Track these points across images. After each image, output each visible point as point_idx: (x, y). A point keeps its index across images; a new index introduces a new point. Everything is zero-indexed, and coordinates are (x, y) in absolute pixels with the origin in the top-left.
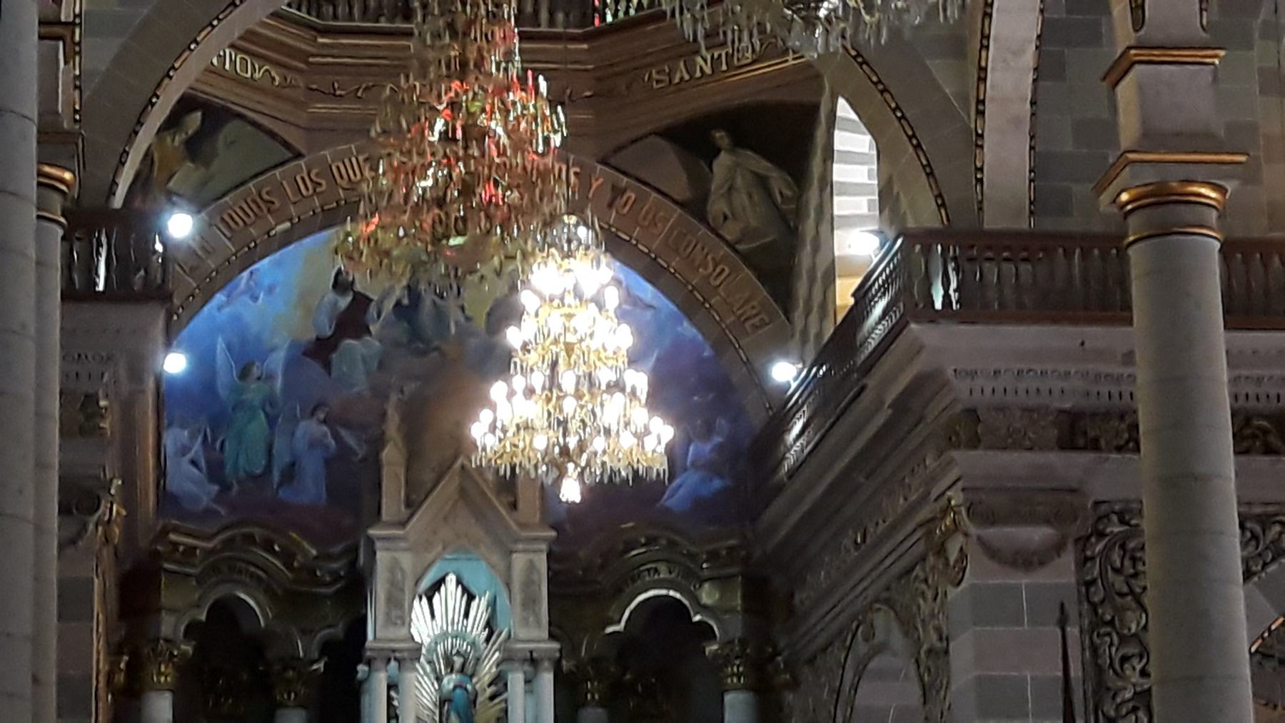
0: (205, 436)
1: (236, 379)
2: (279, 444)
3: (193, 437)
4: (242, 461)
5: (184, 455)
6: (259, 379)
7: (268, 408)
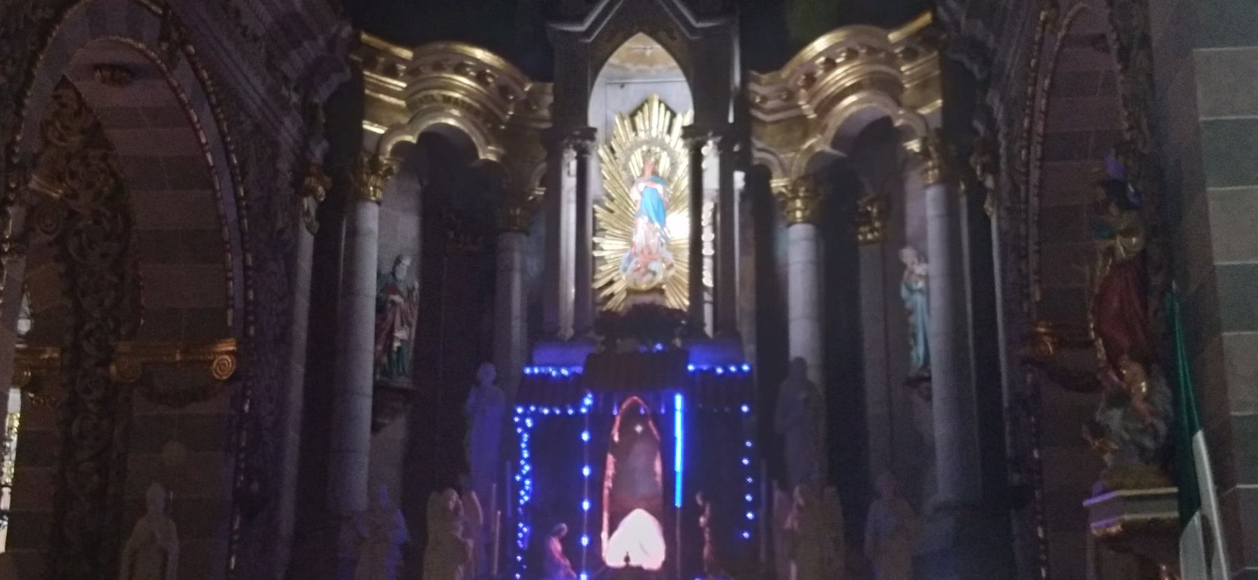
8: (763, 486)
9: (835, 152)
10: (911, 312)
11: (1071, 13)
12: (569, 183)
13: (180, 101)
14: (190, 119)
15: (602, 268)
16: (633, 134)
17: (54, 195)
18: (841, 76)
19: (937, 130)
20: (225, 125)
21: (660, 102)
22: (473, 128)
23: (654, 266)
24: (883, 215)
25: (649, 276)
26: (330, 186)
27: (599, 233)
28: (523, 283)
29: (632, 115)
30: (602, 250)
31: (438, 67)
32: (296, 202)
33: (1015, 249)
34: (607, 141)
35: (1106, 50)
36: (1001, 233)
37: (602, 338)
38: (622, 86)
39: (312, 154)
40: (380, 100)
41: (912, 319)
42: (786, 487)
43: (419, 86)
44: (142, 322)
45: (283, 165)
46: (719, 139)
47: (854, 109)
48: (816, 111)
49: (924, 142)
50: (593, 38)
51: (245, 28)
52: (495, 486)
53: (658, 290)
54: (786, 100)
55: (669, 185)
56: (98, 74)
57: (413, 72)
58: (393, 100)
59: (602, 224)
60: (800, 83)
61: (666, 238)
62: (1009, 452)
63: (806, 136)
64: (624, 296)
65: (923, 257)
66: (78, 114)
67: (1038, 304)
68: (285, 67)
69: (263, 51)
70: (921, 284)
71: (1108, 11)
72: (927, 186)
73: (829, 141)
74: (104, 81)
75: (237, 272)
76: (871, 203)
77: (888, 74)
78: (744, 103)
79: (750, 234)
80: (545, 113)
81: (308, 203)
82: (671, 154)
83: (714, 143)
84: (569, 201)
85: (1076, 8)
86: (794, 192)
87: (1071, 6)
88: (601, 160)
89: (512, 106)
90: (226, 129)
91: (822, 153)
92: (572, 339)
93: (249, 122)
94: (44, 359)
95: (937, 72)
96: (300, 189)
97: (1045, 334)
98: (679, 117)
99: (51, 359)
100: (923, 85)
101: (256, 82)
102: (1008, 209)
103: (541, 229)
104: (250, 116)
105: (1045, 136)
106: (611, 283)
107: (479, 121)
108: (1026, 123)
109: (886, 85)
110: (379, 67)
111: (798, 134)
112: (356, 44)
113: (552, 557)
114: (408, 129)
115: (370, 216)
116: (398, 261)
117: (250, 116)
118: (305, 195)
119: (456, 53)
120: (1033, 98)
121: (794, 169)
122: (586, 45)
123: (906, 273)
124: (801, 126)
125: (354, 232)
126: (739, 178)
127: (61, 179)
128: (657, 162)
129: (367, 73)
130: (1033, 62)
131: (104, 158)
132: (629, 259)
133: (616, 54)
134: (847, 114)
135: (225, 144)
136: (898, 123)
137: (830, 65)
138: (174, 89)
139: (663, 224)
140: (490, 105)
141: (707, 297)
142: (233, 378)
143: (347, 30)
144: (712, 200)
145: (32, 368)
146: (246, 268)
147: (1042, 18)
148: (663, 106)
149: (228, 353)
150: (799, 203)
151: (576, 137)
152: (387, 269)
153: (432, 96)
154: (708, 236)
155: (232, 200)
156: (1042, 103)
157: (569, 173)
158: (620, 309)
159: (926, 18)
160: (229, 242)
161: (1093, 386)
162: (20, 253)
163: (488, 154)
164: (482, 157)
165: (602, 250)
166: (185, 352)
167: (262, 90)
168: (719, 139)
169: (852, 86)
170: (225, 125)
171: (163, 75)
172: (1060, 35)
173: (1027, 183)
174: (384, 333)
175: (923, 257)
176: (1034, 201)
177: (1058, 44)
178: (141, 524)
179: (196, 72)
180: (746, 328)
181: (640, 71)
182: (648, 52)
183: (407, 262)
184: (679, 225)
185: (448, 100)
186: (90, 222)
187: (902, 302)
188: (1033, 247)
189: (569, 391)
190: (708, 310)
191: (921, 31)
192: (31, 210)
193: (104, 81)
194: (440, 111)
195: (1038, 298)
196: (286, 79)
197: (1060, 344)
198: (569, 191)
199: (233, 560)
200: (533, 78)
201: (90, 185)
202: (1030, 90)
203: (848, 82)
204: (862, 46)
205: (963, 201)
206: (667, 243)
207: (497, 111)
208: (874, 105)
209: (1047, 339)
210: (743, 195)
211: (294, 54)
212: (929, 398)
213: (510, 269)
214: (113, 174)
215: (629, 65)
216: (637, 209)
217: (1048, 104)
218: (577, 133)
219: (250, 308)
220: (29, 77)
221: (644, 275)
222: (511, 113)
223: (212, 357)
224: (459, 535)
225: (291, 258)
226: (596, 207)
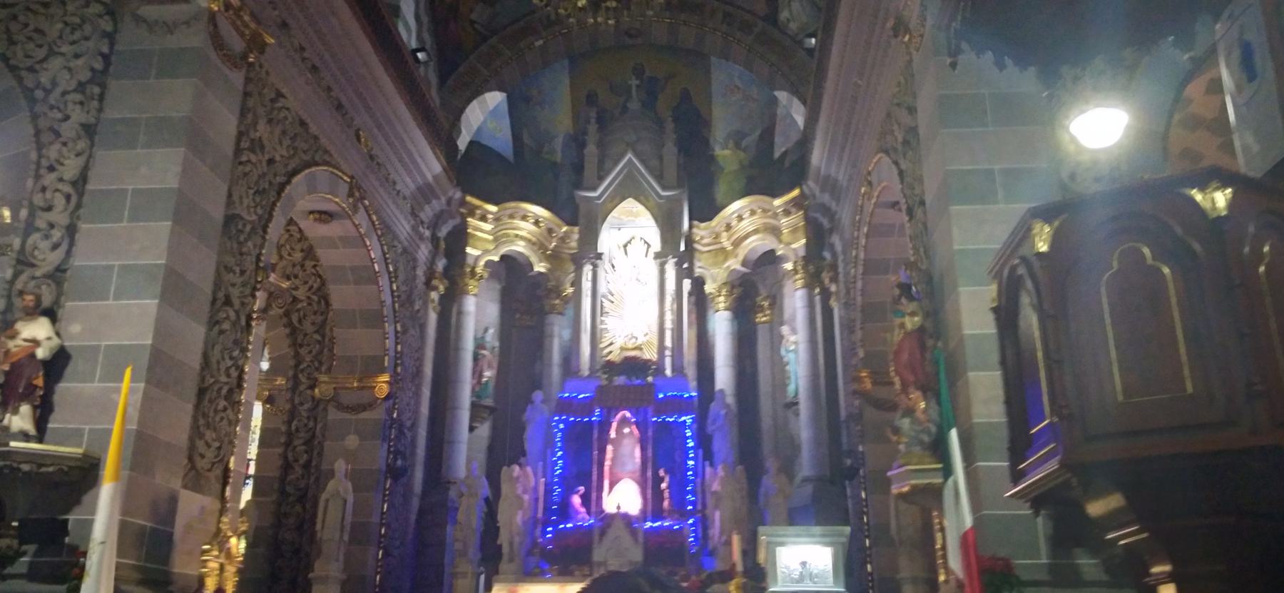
8: (700, 466)
10: (788, 364)
11: (879, 189)
12: (586, 285)
13: (360, 233)
14: (364, 242)
15: (606, 335)
17: (284, 286)
19: (804, 257)
20: (385, 248)
21: (641, 238)
24: (772, 306)
25: (634, 340)
26: (447, 285)
27: (604, 315)
28: (560, 344)
29: (625, 246)
31: (512, 217)
32: (427, 295)
33: (848, 328)
34: (610, 261)
35: (900, 210)
36: (841, 318)
37: (606, 376)
38: (619, 229)
39: (437, 266)
40: (476, 235)
41: (788, 368)
42: (712, 465)
43: (499, 228)
44: (335, 363)
45: (420, 272)
46: (676, 260)
47: (754, 244)
48: (732, 244)
49: (795, 262)
50: (602, 200)
51: (399, 192)
52: (541, 463)
53: (639, 348)
56: (311, 216)
57: (497, 219)
59: (606, 310)
60: (723, 229)
62: (845, 447)
63: (726, 259)
64: (619, 352)
65: (794, 331)
66: (300, 240)
67: (862, 359)
68: (422, 215)
69: (409, 205)
70: (792, 347)
71: (900, 186)
73: (740, 262)
74: (315, 220)
75: (391, 335)
76: (764, 299)
78: (690, 242)
79: (694, 316)
80: (574, 244)
81: (434, 295)
84: (587, 296)
85: (883, 185)
86: (719, 291)
87: (879, 185)
88: (607, 273)
89: (555, 239)
90: (386, 251)
91: (734, 270)
92: (589, 376)
93: (400, 246)
94: (276, 385)
96: (429, 285)
97: (865, 377)
99: (279, 385)
100: (794, 230)
101: (404, 223)
103: (570, 312)
104: (400, 242)
105: (865, 260)
106: (611, 344)
107: (535, 248)
108: (854, 253)
109: (775, 231)
110: (478, 216)
111: (721, 258)
112: (463, 203)
113: (573, 507)
114: (493, 252)
115: (470, 304)
116: (486, 330)
117: (400, 242)
119: (519, 208)
120: (858, 238)
121: (719, 279)
122: (597, 204)
123: (784, 341)
124: (723, 254)
125: (460, 313)
126: (687, 284)
127: (288, 278)
129: (469, 219)
130: (857, 218)
134: (750, 247)
135: (386, 259)
136: (779, 253)
137: (740, 218)
138: (356, 226)
140: (541, 238)
141: (668, 353)
142: (388, 397)
143: (458, 195)
144: (671, 296)
145: (269, 390)
146: (396, 332)
147: (863, 191)
148: (643, 240)
149: (384, 382)
150: (722, 299)
151: (592, 258)
152: (480, 335)
155: (389, 293)
156: (863, 241)
158: (616, 359)
159: (796, 192)
160: (386, 317)
161: (893, 407)
162: (263, 319)
163: (540, 267)
166: (360, 380)
167: (408, 227)
168: (675, 260)
170: (385, 248)
171: (350, 218)
172: (873, 201)
173: (855, 288)
174: (478, 373)
176: (859, 299)
177: (872, 206)
178: (331, 485)
180: (691, 372)
181: (629, 221)
182: (634, 210)
183: (491, 331)
185: (517, 236)
186: (305, 304)
187: (781, 358)
188: (858, 325)
189: (587, 407)
190: (668, 362)
191: (794, 199)
192: (270, 294)
193: (315, 220)
194: (512, 242)
195: (861, 354)
196: (422, 222)
197: (875, 383)
199: (385, 506)
200: (568, 224)
201: (306, 283)
202: (856, 234)
203: (751, 229)
204: (759, 208)
205: (818, 298)
207: (546, 243)
208: (766, 242)
209: (866, 380)
210: (690, 294)
211: (427, 208)
212: (797, 415)
213: (551, 336)
214: (320, 276)
215: (623, 217)
217: (866, 243)
218: (592, 256)
219: (398, 355)
220: (271, 216)
221: (630, 339)
223: (375, 385)
224: (519, 491)
225: (423, 327)
226: (604, 300)
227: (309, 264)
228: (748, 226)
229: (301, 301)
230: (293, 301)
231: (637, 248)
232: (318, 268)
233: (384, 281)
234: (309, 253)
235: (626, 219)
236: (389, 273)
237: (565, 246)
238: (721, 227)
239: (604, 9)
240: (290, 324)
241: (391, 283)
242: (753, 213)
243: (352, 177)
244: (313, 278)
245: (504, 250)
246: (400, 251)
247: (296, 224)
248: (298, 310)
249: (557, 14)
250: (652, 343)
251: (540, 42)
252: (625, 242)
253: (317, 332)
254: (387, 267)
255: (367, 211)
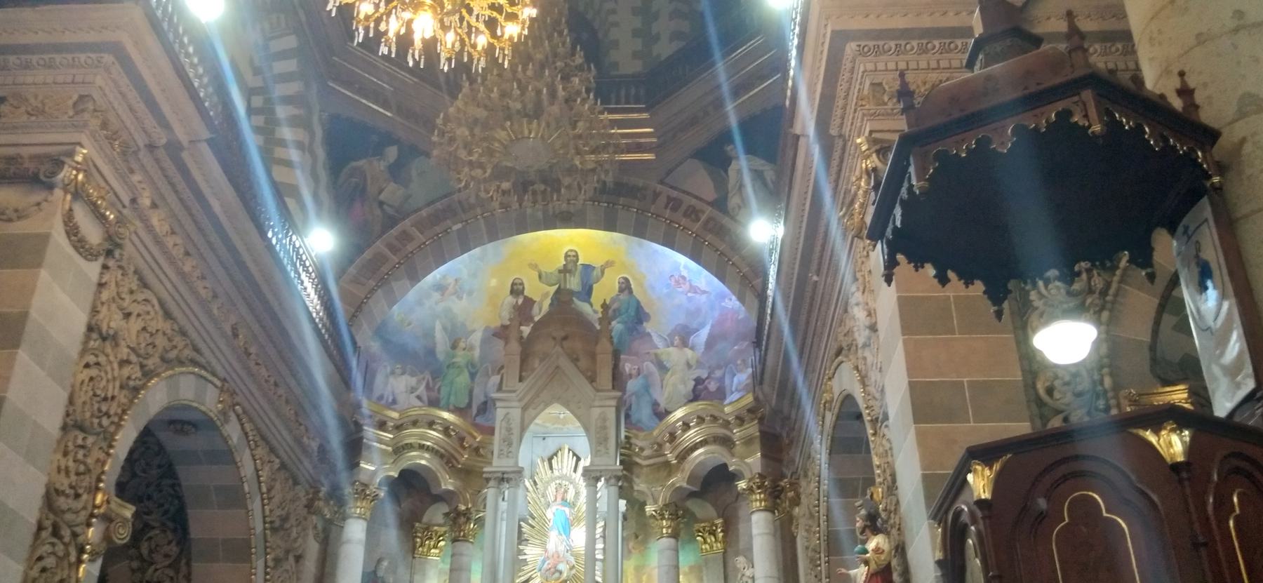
0: (428, 381)
1: (449, 349)
2: (476, 391)
3: (419, 382)
4: (452, 398)
5: (412, 393)
6: (464, 349)
7: (470, 367)
9: (689, 487)
15: (525, 568)
16: (549, 472)
18: (693, 435)
19: (759, 474)
21: (569, 450)
22: (438, 467)
23: (561, 567)
25: (557, 575)
27: (524, 543)
29: (550, 460)
30: (525, 554)
34: (532, 477)
38: (544, 439)
47: (702, 457)
49: (750, 480)
54: (656, 451)
55: (574, 508)
58: (383, 447)
61: (570, 546)
63: (670, 475)
72: (753, 512)
73: (686, 479)
77: (727, 435)
82: (576, 488)
83: (605, 479)
88: (527, 489)
91: (680, 488)
93: (277, 461)
95: (758, 434)
98: (582, 460)
102: (807, 531)
104: (278, 457)
109: (726, 442)
118: (314, 513)
123: (739, 576)
126: (622, 504)
128: (566, 491)
131: (173, 486)
132: (544, 562)
133: (539, 417)
134: (697, 461)
135: (259, 477)
136: (731, 469)
137: (686, 426)
139: (568, 536)
140: (453, 452)
146: (266, 567)
153: (411, 444)
154: (600, 546)
157: (503, 499)
164: (444, 487)
165: (525, 554)
169: (701, 441)
173: (819, 512)
175: (751, 564)
179: (242, 425)
181: (556, 428)
184: (579, 537)
186: (158, 532)
198: (503, 512)
204: (707, 416)
206: (570, 550)
207: (456, 455)
208: (716, 455)
214: (180, 498)
215: (548, 425)
216: (550, 524)
221: (554, 573)
222: (466, 456)
226: (522, 523)
227: (169, 482)
228: (695, 436)
229: (153, 528)
230: (143, 530)
231: (565, 463)
232: (177, 488)
233: (256, 506)
234: (169, 471)
235: (553, 427)
236: (262, 494)
237: (480, 459)
238: (664, 436)
239: (530, 193)
240: (140, 557)
241: (263, 505)
242: (701, 420)
243: (224, 380)
244: (170, 499)
245: (405, 464)
246: (277, 466)
247: (153, 435)
248: (150, 538)
249: (477, 196)
250: (579, 578)
251: (455, 228)
252: (549, 453)
253: (169, 566)
254: (260, 488)
255: (240, 420)
